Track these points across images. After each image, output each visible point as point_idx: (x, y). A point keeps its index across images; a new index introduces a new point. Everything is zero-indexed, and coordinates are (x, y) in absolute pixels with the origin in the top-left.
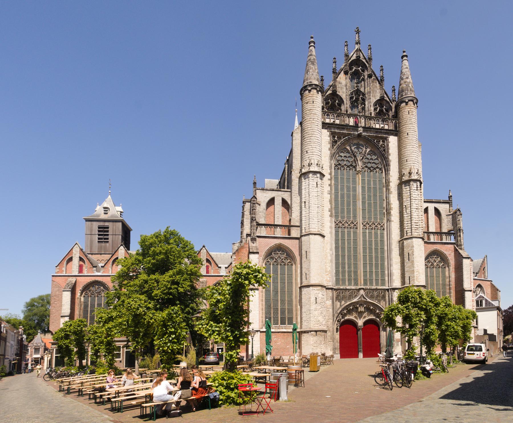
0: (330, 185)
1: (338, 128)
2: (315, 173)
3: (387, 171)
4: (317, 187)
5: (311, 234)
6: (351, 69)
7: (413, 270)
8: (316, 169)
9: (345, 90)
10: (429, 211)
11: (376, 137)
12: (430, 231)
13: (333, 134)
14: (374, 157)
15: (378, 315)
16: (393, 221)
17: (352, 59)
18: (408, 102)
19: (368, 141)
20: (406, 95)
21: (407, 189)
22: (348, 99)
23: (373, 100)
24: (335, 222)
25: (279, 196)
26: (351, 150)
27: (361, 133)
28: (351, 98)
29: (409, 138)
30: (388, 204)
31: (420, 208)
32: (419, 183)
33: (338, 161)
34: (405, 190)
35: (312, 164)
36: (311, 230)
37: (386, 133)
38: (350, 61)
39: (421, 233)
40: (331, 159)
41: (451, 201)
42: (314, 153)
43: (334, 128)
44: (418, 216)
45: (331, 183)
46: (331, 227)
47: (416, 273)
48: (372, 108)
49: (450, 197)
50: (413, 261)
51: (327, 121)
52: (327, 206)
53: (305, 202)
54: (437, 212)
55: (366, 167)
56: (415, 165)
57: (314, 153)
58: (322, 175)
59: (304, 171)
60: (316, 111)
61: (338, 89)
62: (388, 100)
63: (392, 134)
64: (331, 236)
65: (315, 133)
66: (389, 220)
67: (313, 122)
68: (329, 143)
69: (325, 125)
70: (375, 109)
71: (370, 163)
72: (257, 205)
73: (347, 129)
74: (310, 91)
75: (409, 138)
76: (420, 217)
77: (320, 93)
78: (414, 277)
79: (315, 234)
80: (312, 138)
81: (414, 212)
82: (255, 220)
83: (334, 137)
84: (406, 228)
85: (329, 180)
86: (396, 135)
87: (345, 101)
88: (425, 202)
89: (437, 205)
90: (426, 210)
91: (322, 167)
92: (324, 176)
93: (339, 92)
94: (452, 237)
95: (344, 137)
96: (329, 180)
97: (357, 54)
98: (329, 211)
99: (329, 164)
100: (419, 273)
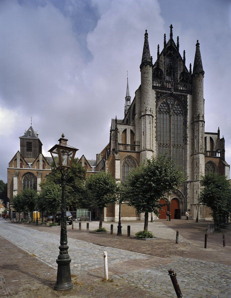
0: (156, 123)
1: (160, 89)
2: (149, 115)
3: (186, 115)
4: (150, 124)
5: (147, 150)
6: (167, 52)
7: (199, 172)
8: (150, 113)
9: (164, 66)
10: (207, 139)
11: (181, 95)
12: (207, 150)
13: (157, 93)
14: (178, 107)
15: (179, 196)
16: (188, 144)
17: (168, 46)
18: (199, 74)
19: (176, 97)
20: (198, 69)
21: (197, 126)
22: (165, 72)
23: (179, 72)
24: (158, 144)
25: (129, 128)
26: (167, 102)
27: (173, 93)
28: (167, 71)
29: (199, 96)
30: (186, 134)
31: (203, 137)
32: (203, 122)
33: (160, 109)
34: (195, 127)
35: (147, 110)
36: (147, 148)
37: (186, 93)
38: (167, 47)
39: (203, 151)
40: (156, 108)
41: (219, 133)
42: (148, 104)
43: (158, 89)
44: (201, 141)
45: (156, 122)
46: (156, 147)
47: (200, 174)
48: (179, 77)
49: (219, 131)
50: (199, 167)
51: (155, 85)
52: (155, 135)
53: (143, 132)
54: (211, 139)
55: (175, 113)
56: (202, 112)
57: (148, 104)
58: (153, 117)
59: (143, 114)
60: (149, 78)
61: (160, 65)
62: (187, 72)
63: (189, 93)
64: (156, 152)
65: (149, 92)
66: (186, 144)
67: (148, 85)
68: (155, 98)
69: (154, 87)
70: (180, 78)
71: (177, 110)
72: (118, 133)
73: (166, 90)
74: (146, 66)
75: (199, 96)
76: (203, 142)
77: (151, 67)
78: (199, 176)
79: (149, 150)
80: (147, 95)
81: (200, 139)
82: (118, 141)
83: (158, 94)
84: (196, 148)
85: (155, 119)
86: (191, 94)
87: (164, 72)
88: (205, 134)
89: (211, 136)
90: (206, 138)
91: (152, 112)
92: (153, 117)
93: (161, 67)
94: (219, 154)
95: (163, 95)
96: (155, 119)
97: (170, 43)
98: (155, 138)
99: (155, 111)
100: (202, 173)
